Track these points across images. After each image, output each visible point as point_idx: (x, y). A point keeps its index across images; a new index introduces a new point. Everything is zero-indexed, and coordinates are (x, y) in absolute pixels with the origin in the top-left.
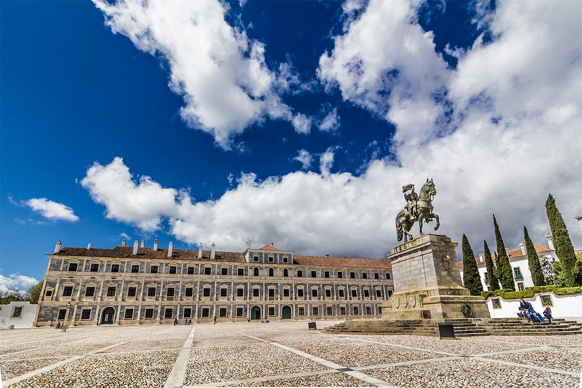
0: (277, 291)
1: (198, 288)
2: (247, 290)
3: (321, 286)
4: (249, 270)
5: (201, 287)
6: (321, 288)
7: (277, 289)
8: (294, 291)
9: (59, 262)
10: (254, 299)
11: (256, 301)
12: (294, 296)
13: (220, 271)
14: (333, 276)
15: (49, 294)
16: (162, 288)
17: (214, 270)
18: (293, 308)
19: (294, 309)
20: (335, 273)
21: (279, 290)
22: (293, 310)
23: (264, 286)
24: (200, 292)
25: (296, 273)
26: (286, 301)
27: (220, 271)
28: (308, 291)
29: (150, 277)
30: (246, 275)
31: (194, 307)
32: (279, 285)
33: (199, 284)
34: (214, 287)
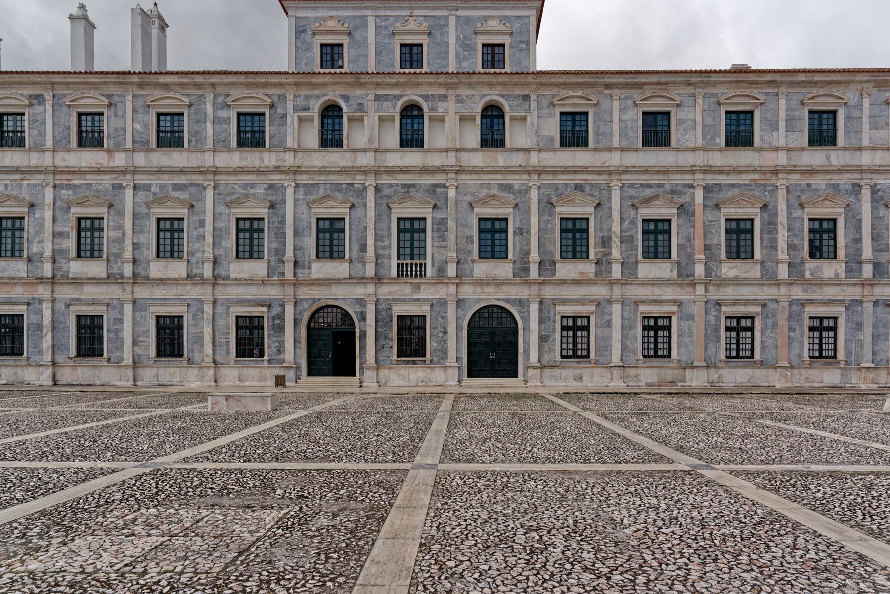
1: (48, 214)
2: (283, 222)
3: (699, 196)
4: (292, 119)
5: (61, 208)
6: (699, 211)
7: (439, 215)
8: (534, 230)
11: (335, 283)
12: (534, 255)
13: (146, 126)
14: (780, 138)
17: (119, 123)
18: (526, 320)
19: (534, 325)
20: (789, 121)
21: (451, 224)
22: (526, 328)
25: (552, 128)
26: (492, 283)
27: (146, 126)
28: (616, 228)
30: (280, 147)
31: (36, 306)
32: (452, 193)
33: (49, 194)
34: (121, 214)
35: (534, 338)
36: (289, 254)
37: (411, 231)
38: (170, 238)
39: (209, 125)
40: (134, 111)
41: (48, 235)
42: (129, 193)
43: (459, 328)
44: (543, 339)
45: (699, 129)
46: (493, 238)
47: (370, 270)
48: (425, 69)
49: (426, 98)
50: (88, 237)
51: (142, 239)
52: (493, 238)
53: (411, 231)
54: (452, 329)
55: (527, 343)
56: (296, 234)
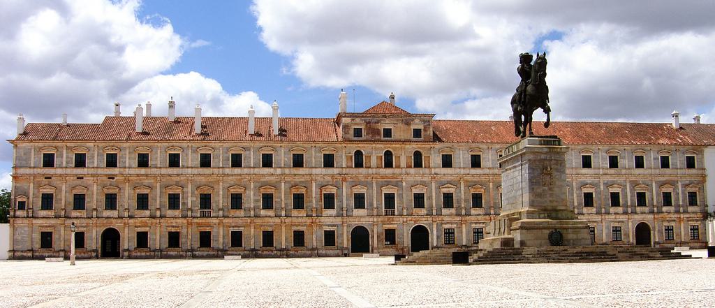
0: (401, 196)
1: (252, 193)
8: (434, 197)
9: (27, 153)
10: (357, 212)
11: (361, 217)
15: (22, 206)
16: (190, 195)
19: (435, 232)
23: (375, 188)
24: (255, 201)
28: (463, 197)
29: (170, 175)
35: (435, 237)
36: (345, 206)
37: (390, 199)
38: (299, 201)
39: (313, 159)
40: (285, 154)
41: (252, 201)
42: (283, 184)
43: (408, 233)
44: (438, 237)
45: (490, 161)
46: (419, 200)
47: (375, 212)
48: (393, 138)
49: (395, 149)
50: (268, 201)
51: (288, 201)
52: (419, 200)
53: (390, 199)
54: (405, 234)
55: (432, 239)
56: (347, 200)
